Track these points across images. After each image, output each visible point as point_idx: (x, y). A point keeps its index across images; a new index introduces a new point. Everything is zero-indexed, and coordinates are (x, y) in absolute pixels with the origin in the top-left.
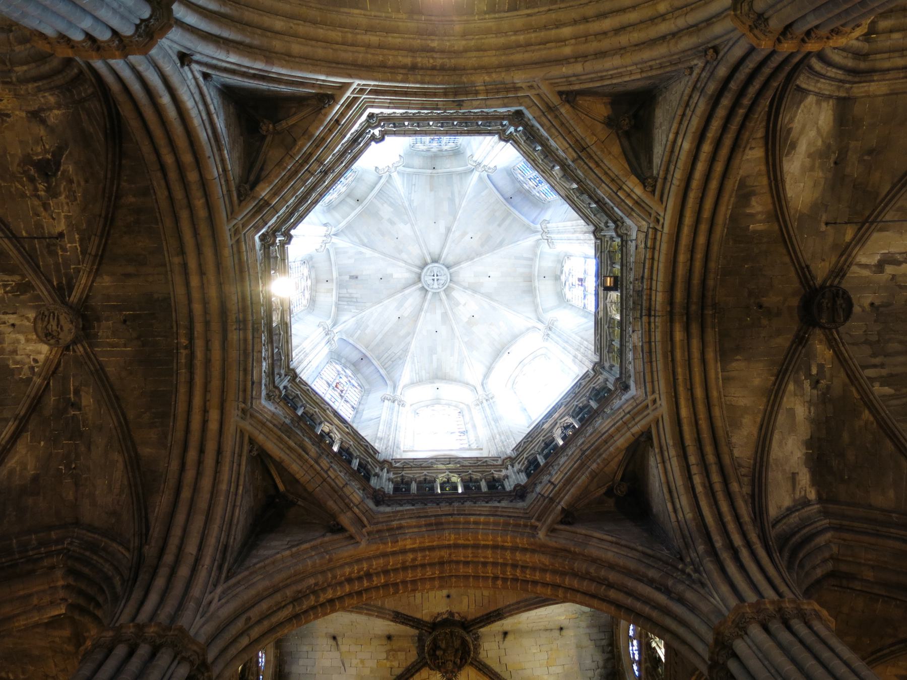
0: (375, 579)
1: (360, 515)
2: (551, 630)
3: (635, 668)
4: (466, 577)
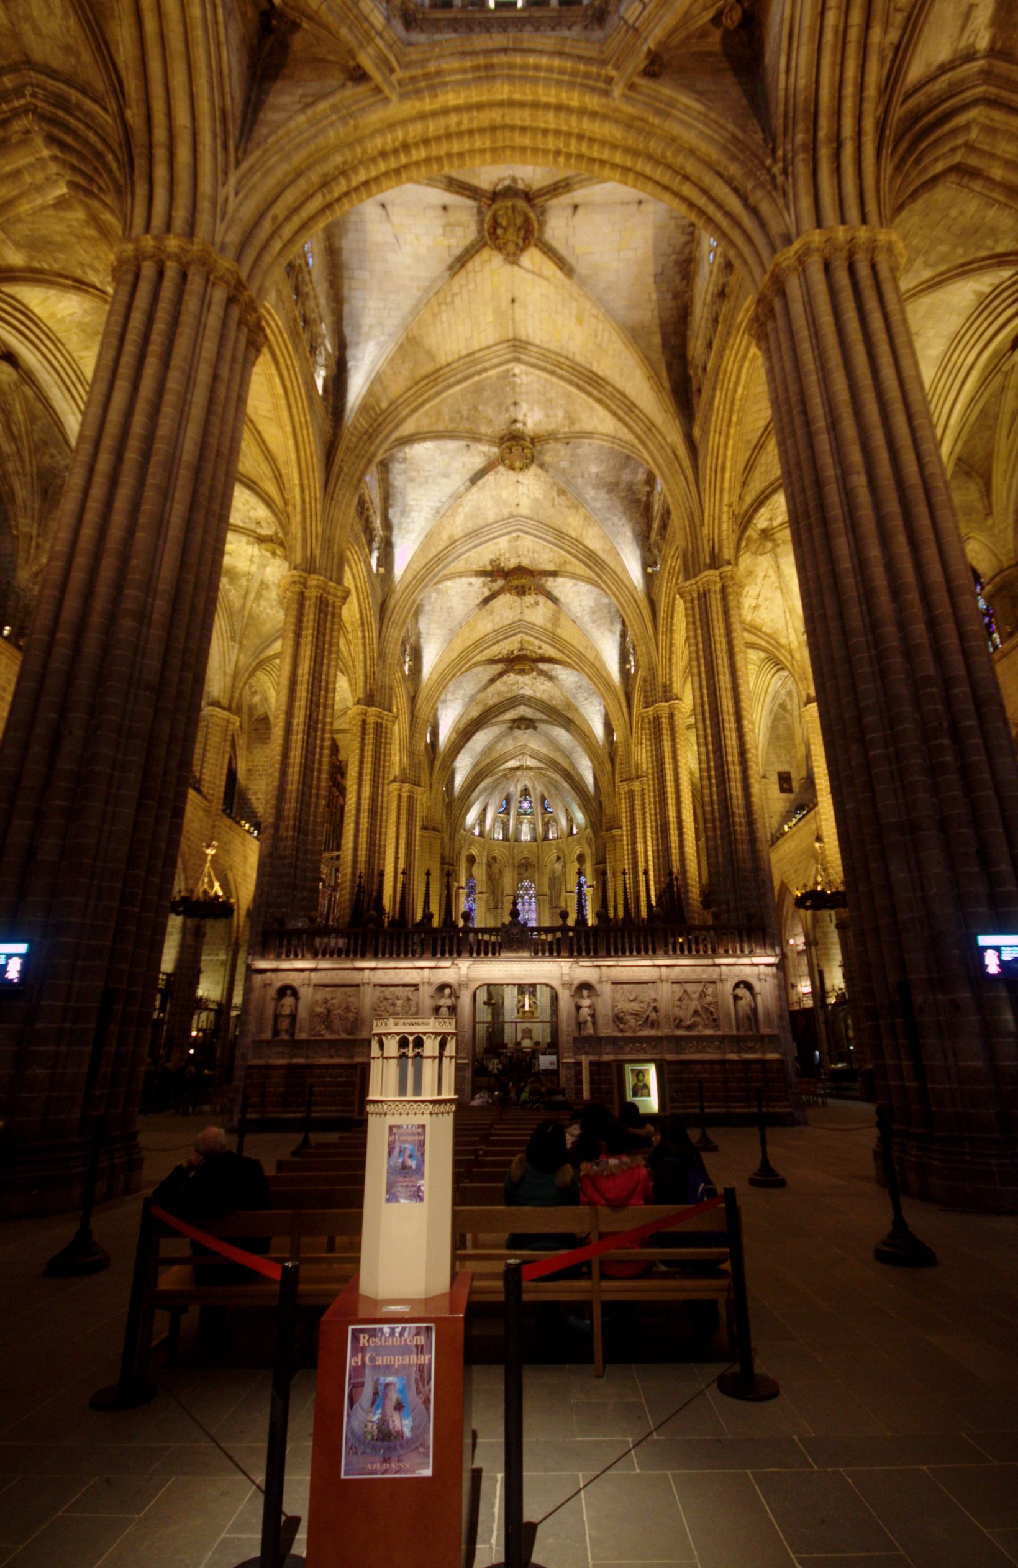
0: (414, 152)
1: (386, 51)
2: (628, 203)
3: (711, 257)
4: (523, 149)
